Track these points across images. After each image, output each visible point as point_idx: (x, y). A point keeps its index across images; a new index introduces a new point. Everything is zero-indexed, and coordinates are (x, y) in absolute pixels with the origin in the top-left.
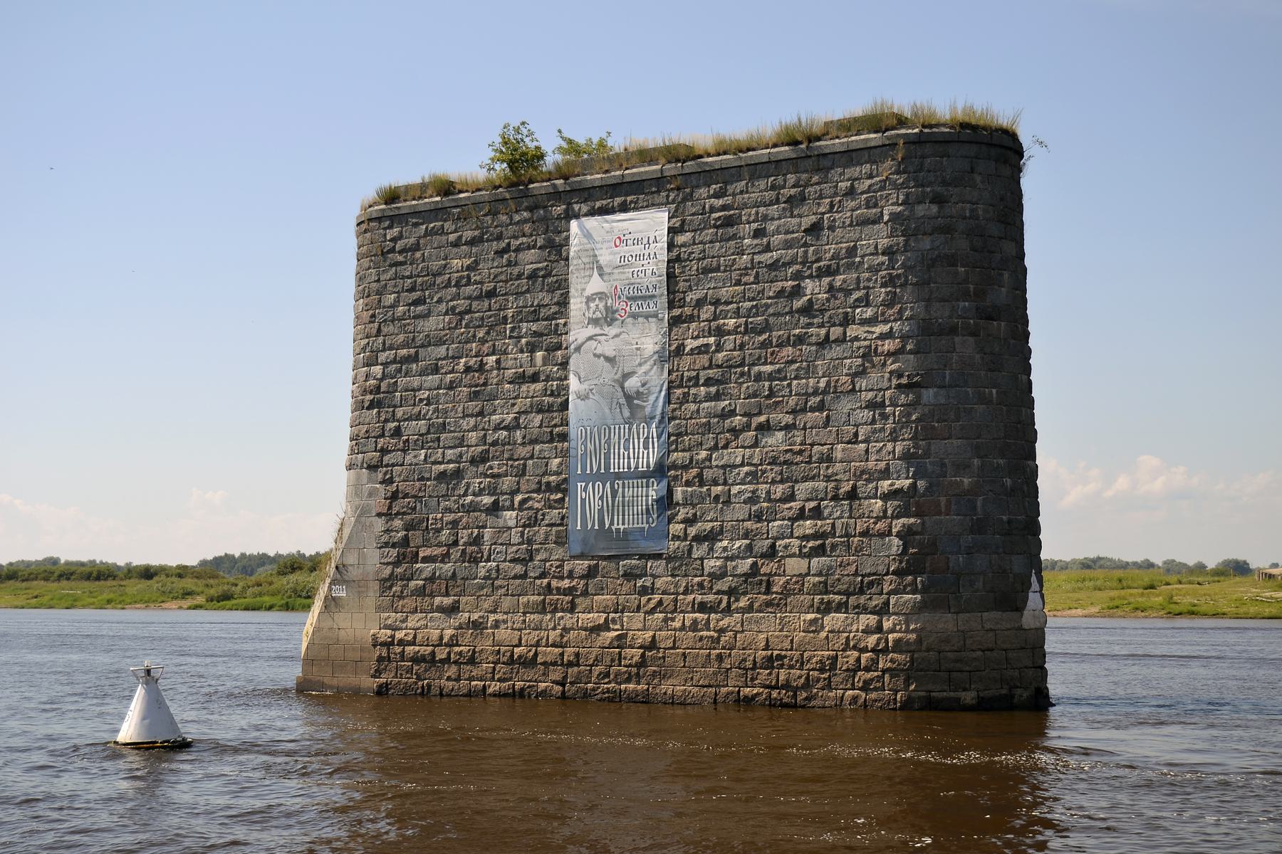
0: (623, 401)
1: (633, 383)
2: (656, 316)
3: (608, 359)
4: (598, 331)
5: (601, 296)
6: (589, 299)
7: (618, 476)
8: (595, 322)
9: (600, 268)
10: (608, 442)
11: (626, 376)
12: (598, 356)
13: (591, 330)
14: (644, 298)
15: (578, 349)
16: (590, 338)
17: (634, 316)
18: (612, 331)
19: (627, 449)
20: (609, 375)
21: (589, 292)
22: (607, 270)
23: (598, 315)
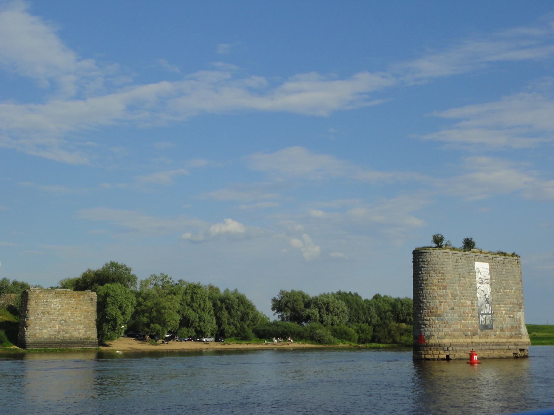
0: (485, 299)
1: (487, 296)
2: (488, 283)
3: (483, 291)
4: (481, 285)
5: (481, 278)
6: (479, 279)
7: (486, 314)
8: (480, 283)
9: (480, 273)
10: (484, 307)
11: (486, 295)
12: (481, 290)
13: (480, 285)
14: (487, 280)
15: (478, 288)
16: (480, 286)
17: (486, 283)
18: (483, 285)
19: (487, 309)
20: (483, 294)
21: (479, 277)
22: (481, 273)
23: (481, 282)
